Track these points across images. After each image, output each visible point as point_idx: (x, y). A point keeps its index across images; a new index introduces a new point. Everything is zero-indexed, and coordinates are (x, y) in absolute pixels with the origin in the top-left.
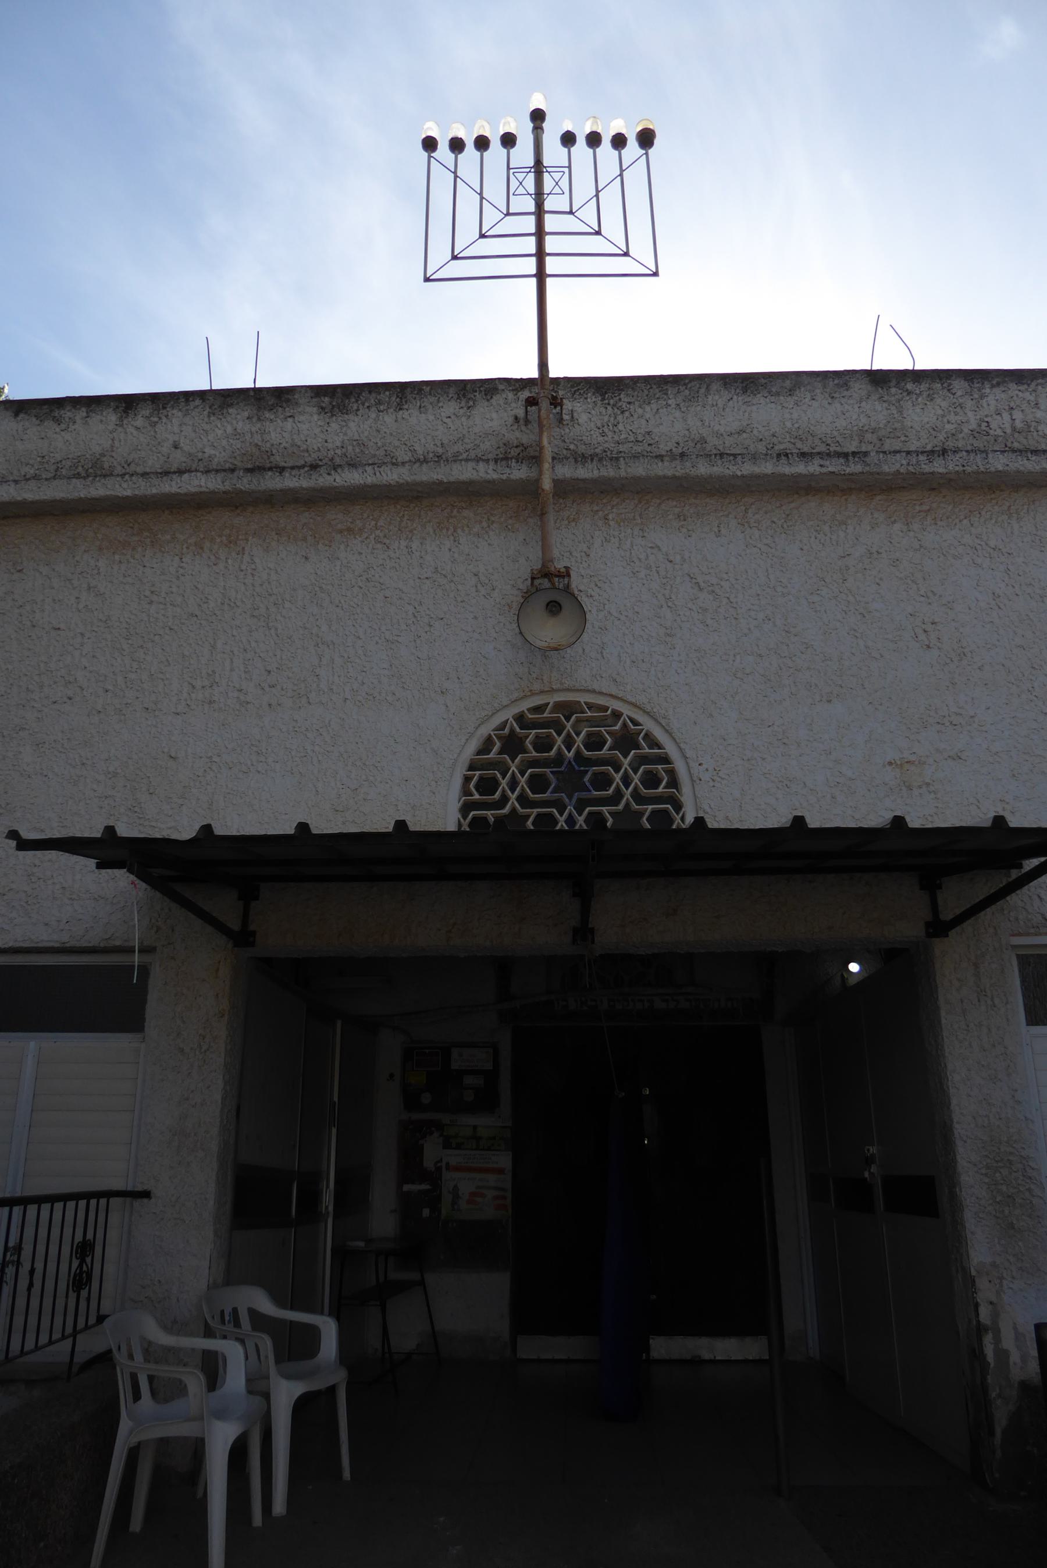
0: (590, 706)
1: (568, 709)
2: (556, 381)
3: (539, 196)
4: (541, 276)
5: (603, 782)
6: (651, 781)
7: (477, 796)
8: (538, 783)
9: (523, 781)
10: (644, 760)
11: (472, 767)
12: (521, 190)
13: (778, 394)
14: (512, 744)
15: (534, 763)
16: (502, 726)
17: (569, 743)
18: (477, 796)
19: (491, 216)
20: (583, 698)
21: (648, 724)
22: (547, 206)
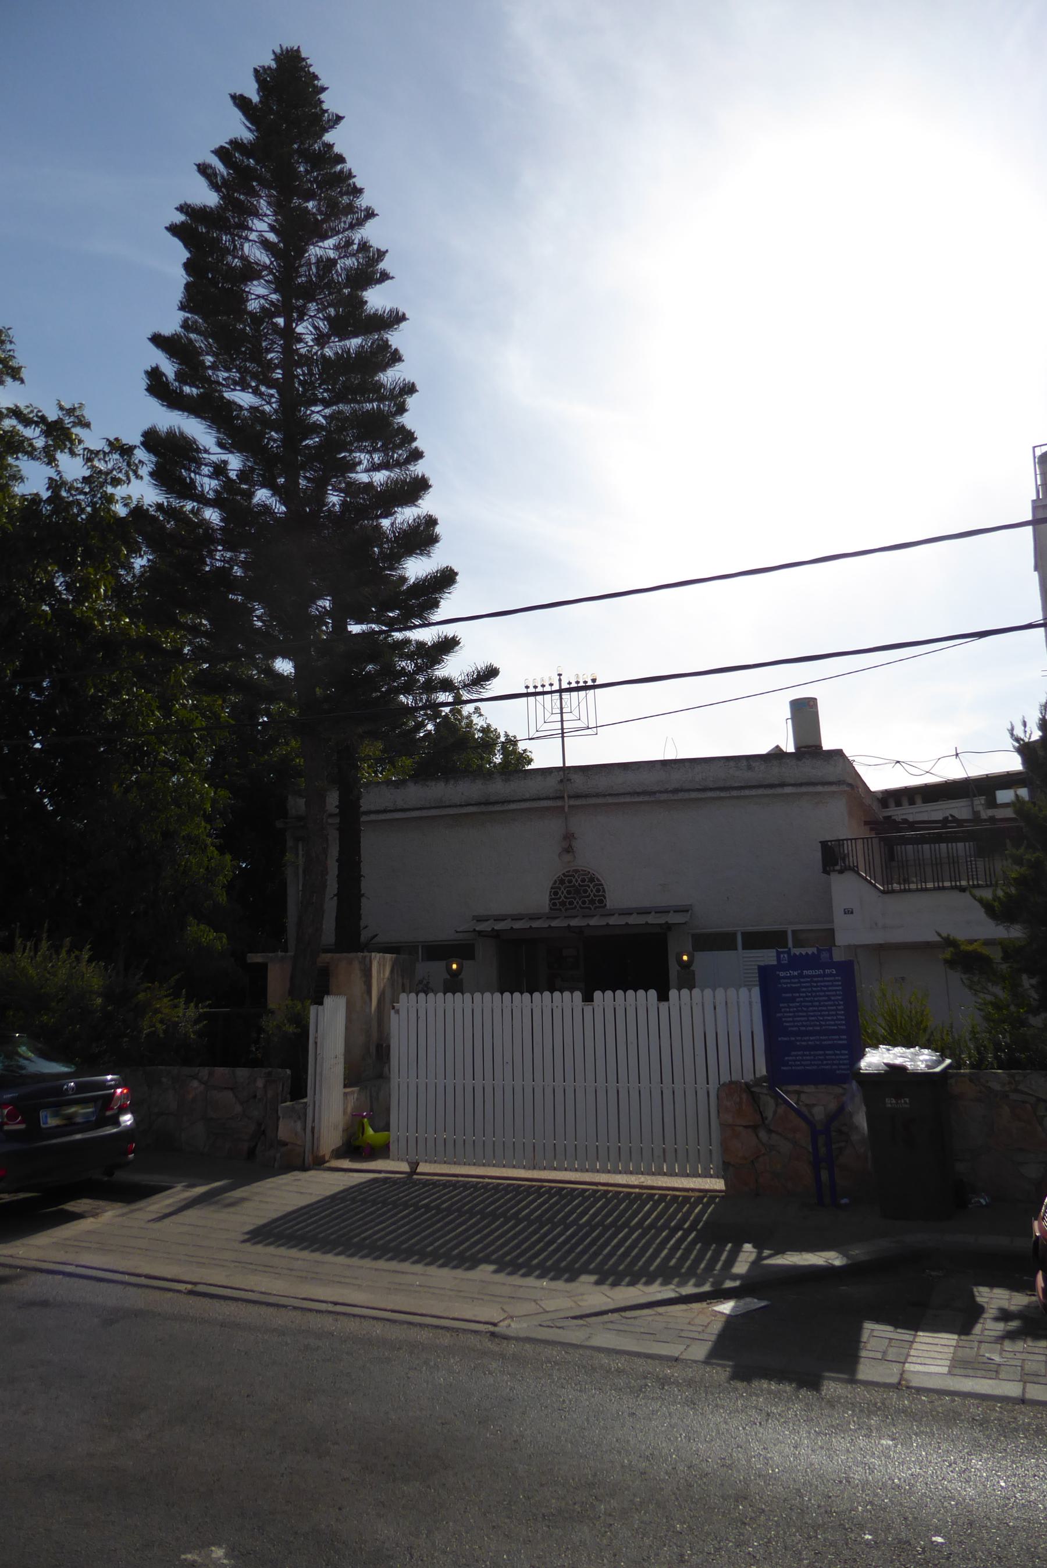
0: (582, 870)
1: (576, 871)
2: (569, 768)
3: (561, 708)
4: (563, 737)
5: (586, 891)
6: (598, 891)
7: (553, 897)
8: (569, 892)
9: (565, 892)
10: (596, 885)
11: (552, 888)
12: (555, 707)
13: (633, 770)
14: (562, 882)
15: (568, 887)
16: (559, 877)
17: (577, 881)
18: (553, 897)
19: (547, 715)
20: (580, 868)
21: (597, 875)
22: (564, 711)
